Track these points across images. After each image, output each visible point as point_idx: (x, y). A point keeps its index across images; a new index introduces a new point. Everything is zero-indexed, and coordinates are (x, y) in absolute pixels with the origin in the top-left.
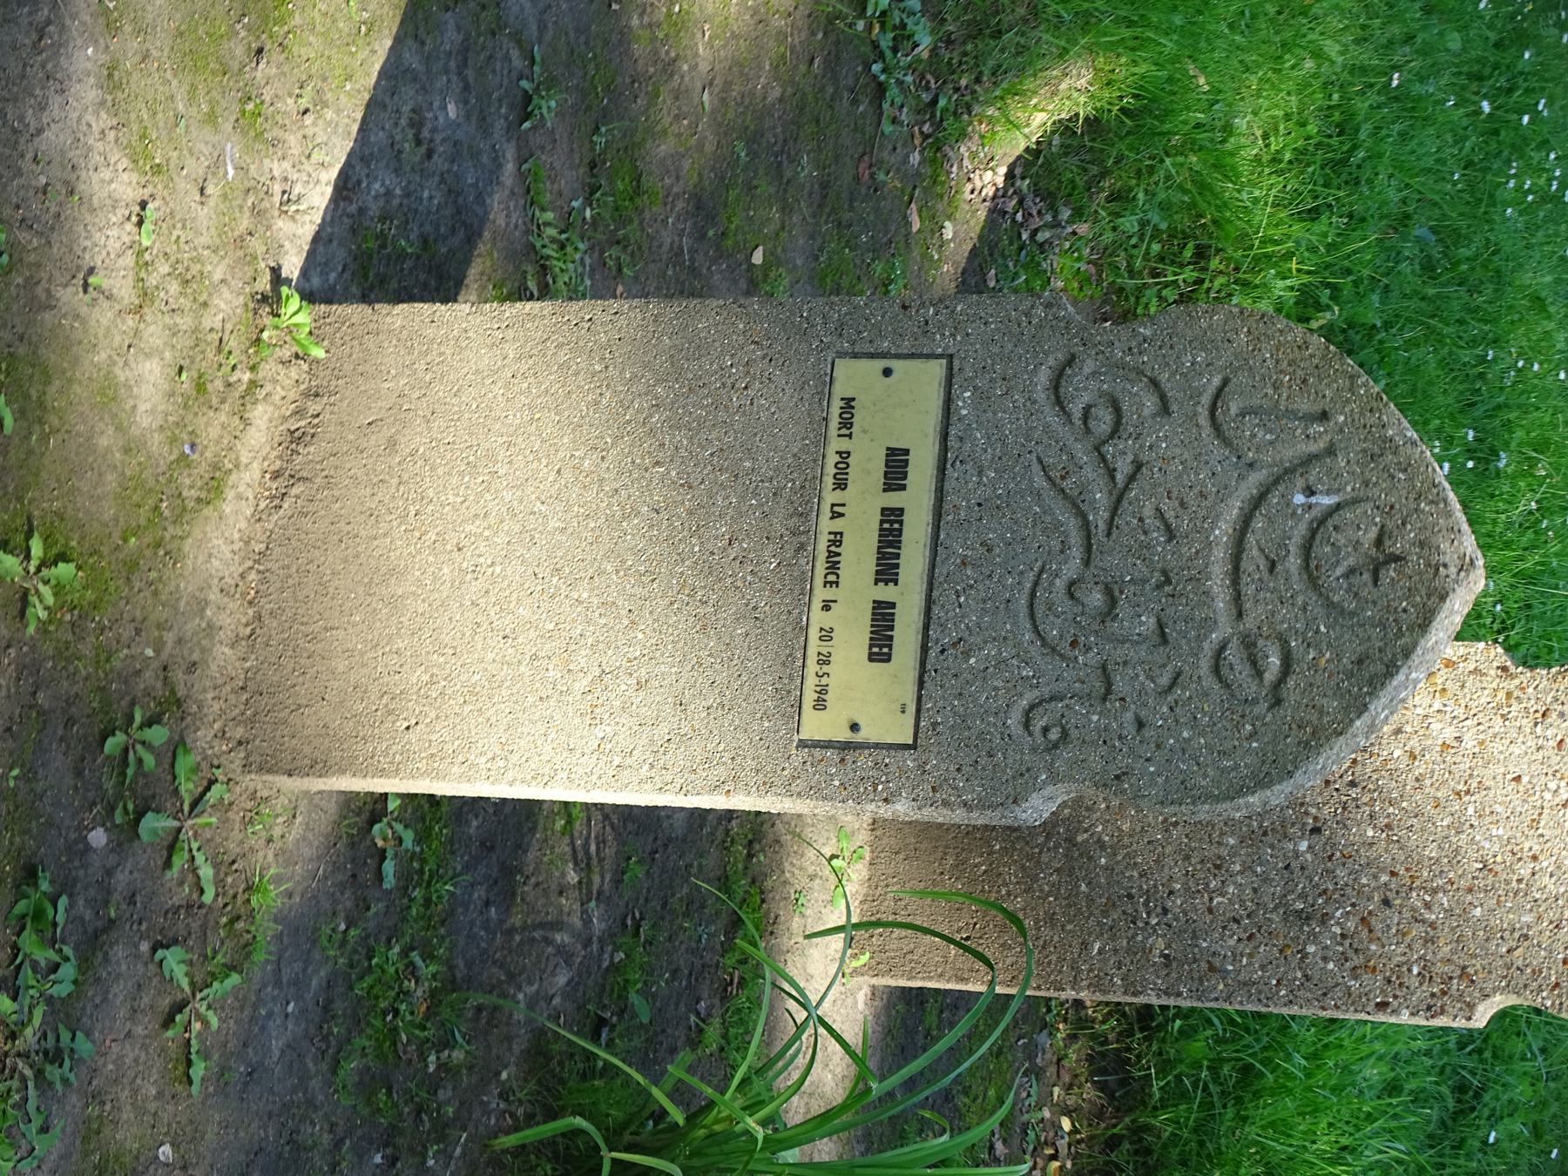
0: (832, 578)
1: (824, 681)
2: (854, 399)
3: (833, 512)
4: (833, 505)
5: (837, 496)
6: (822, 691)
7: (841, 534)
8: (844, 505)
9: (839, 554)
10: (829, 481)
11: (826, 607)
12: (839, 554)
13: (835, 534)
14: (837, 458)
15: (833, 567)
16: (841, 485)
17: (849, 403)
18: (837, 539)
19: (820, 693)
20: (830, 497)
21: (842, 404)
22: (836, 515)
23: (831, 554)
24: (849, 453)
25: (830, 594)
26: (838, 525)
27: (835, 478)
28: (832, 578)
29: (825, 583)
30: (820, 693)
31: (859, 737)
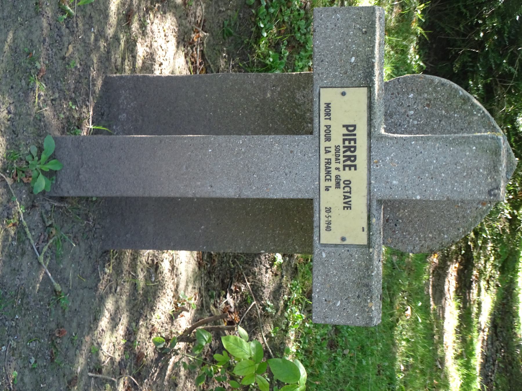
0: (328, 177)
1: (330, 219)
2: (330, 104)
3: (326, 150)
4: (326, 148)
5: (328, 144)
7: (330, 159)
8: (330, 147)
9: (330, 168)
10: (322, 138)
11: (327, 189)
12: (330, 168)
13: (328, 159)
14: (326, 128)
15: (328, 173)
16: (328, 139)
18: (328, 162)
19: (328, 224)
20: (324, 144)
22: (327, 152)
23: (327, 168)
24: (330, 126)
25: (328, 184)
26: (329, 156)
27: (326, 135)
28: (328, 177)
29: (326, 180)
30: (328, 224)
31: (344, 243)
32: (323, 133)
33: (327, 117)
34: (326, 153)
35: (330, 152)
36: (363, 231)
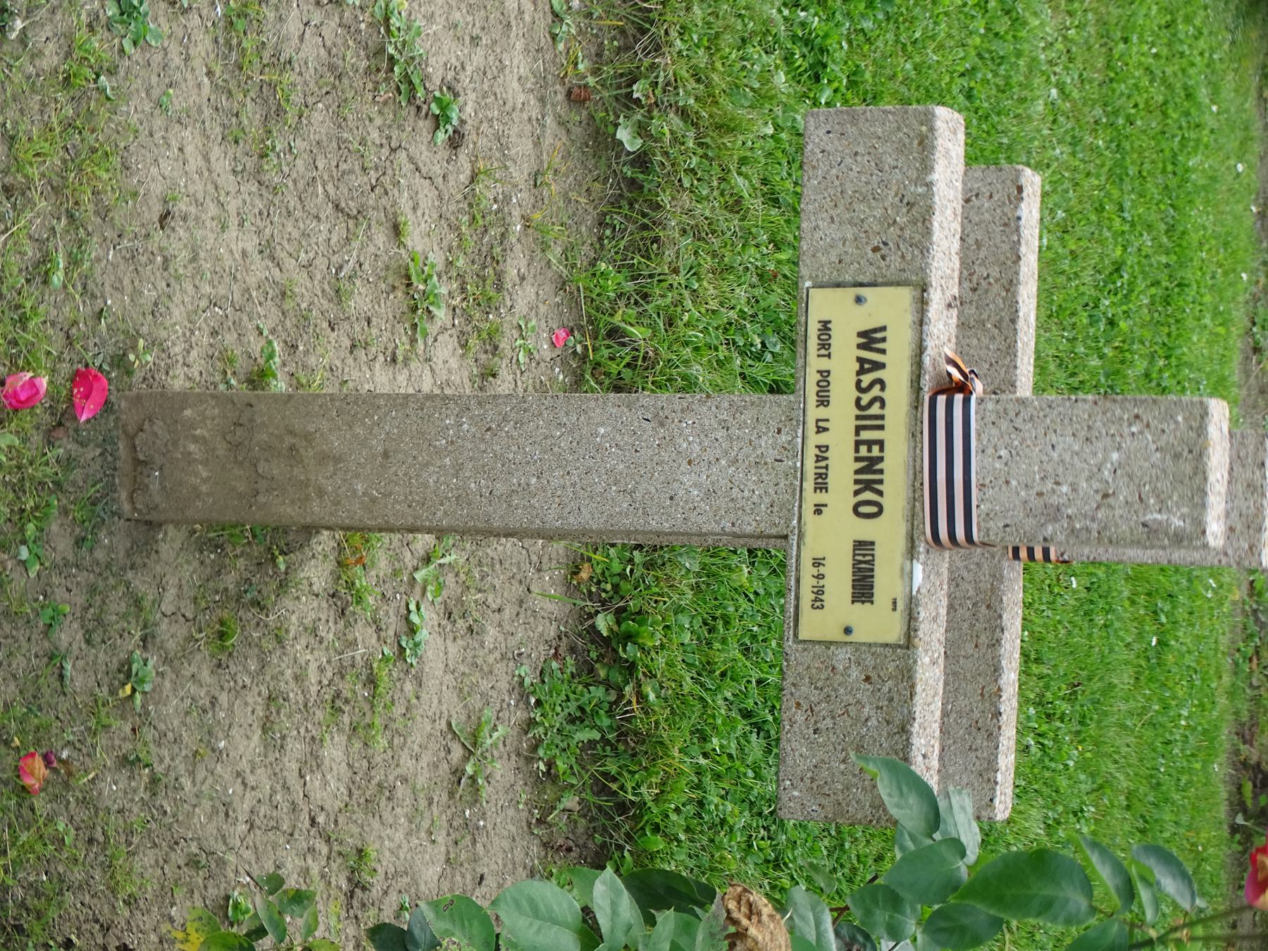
1: (821, 582)
2: (830, 322)
3: (818, 427)
4: (818, 421)
5: (822, 412)
6: (819, 592)
10: (812, 399)
14: (819, 377)
16: (823, 402)
17: (825, 326)
19: (817, 593)
20: (814, 413)
21: (819, 326)
24: (828, 372)
26: (823, 439)
30: (817, 593)
32: (812, 389)
33: (823, 352)
34: (818, 432)
35: (826, 429)
36: (894, 609)
